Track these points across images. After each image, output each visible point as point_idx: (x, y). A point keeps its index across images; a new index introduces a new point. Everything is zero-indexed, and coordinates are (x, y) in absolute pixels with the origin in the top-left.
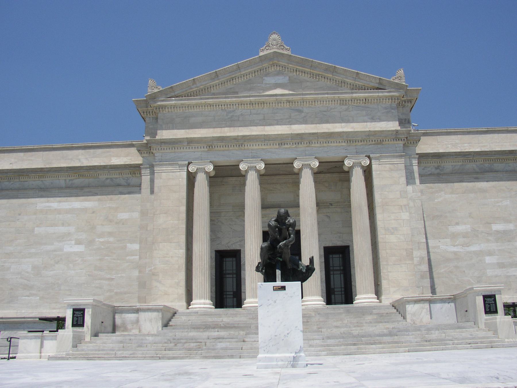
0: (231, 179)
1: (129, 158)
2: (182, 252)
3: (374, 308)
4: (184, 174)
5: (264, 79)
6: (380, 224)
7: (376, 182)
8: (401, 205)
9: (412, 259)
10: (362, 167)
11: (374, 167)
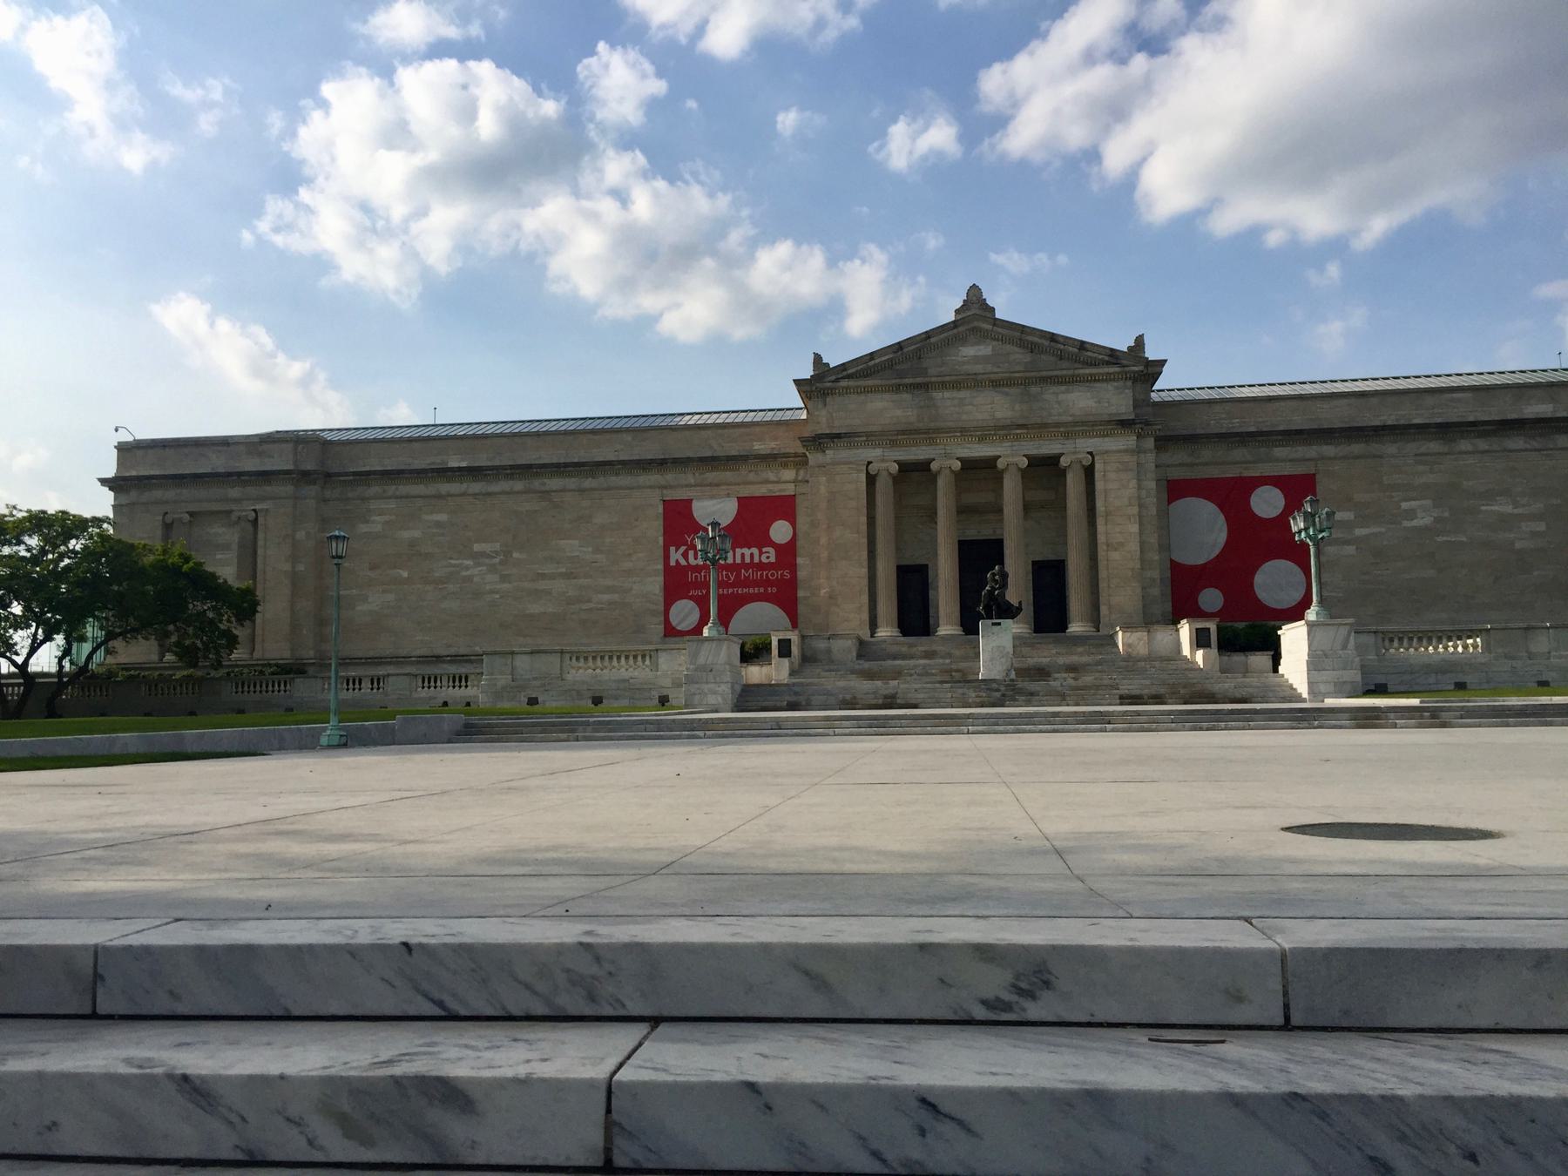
2: (864, 571)
3: (1088, 638)
4: (863, 477)
5: (960, 350)
6: (1101, 538)
7: (1099, 485)
11: (1097, 466)
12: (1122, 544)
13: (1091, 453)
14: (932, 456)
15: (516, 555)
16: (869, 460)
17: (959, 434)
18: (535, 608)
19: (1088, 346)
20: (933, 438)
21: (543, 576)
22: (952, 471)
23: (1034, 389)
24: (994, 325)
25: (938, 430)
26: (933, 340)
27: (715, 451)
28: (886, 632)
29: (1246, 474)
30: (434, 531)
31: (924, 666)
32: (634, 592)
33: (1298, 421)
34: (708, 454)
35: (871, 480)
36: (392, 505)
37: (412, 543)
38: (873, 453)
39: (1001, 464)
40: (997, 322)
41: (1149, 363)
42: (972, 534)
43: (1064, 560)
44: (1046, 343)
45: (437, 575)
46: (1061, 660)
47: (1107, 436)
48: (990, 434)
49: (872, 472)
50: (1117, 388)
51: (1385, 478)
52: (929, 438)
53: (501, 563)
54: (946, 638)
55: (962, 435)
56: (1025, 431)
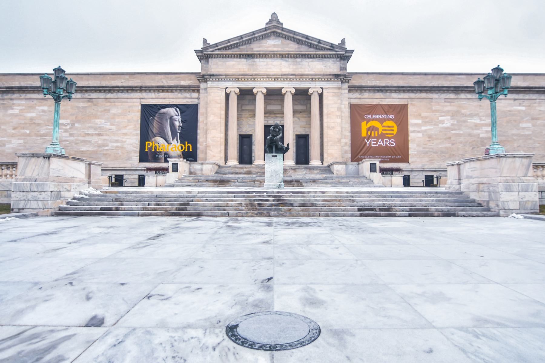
0: (248, 96)
1: (192, 82)
2: (223, 135)
3: (319, 167)
4: (224, 94)
6: (325, 125)
7: (325, 102)
8: (337, 115)
9: (340, 143)
10: (318, 93)
11: (325, 94)
12: (333, 128)
13: (322, 88)
14: (254, 86)
15: (77, 125)
16: (227, 87)
17: (266, 77)
18: (84, 148)
19: (321, 42)
20: (255, 78)
21: (88, 135)
22: (263, 93)
23: (299, 60)
24: (282, 30)
25: (256, 75)
26: (256, 35)
27: (164, 84)
28: (233, 161)
29: (381, 103)
30: (41, 114)
31: (243, 178)
32: (127, 143)
33: (401, 83)
34: (162, 85)
35: (227, 96)
36: (23, 102)
37: (32, 119)
38: (229, 84)
39: (283, 91)
40: (284, 29)
41: (347, 51)
42: (271, 122)
43: (308, 135)
44: (304, 39)
45: (41, 132)
46: (307, 177)
47: (329, 81)
48: (279, 78)
49: (227, 92)
50: (333, 61)
51: (433, 107)
52: (253, 78)
53: (70, 128)
54: (258, 166)
55: (267, 78)
56: (294, 77)
